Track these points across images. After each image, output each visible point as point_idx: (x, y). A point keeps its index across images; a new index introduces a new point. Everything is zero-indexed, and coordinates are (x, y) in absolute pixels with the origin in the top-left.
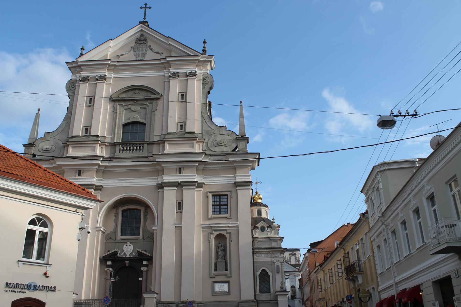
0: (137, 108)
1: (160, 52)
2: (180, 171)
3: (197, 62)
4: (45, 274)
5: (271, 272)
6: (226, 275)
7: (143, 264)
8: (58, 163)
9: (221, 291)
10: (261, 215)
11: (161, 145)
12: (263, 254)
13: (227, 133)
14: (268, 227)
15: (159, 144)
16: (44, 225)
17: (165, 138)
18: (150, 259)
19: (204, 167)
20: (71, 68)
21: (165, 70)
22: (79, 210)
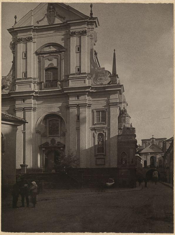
11: (67, 82)
15: (66, 81)
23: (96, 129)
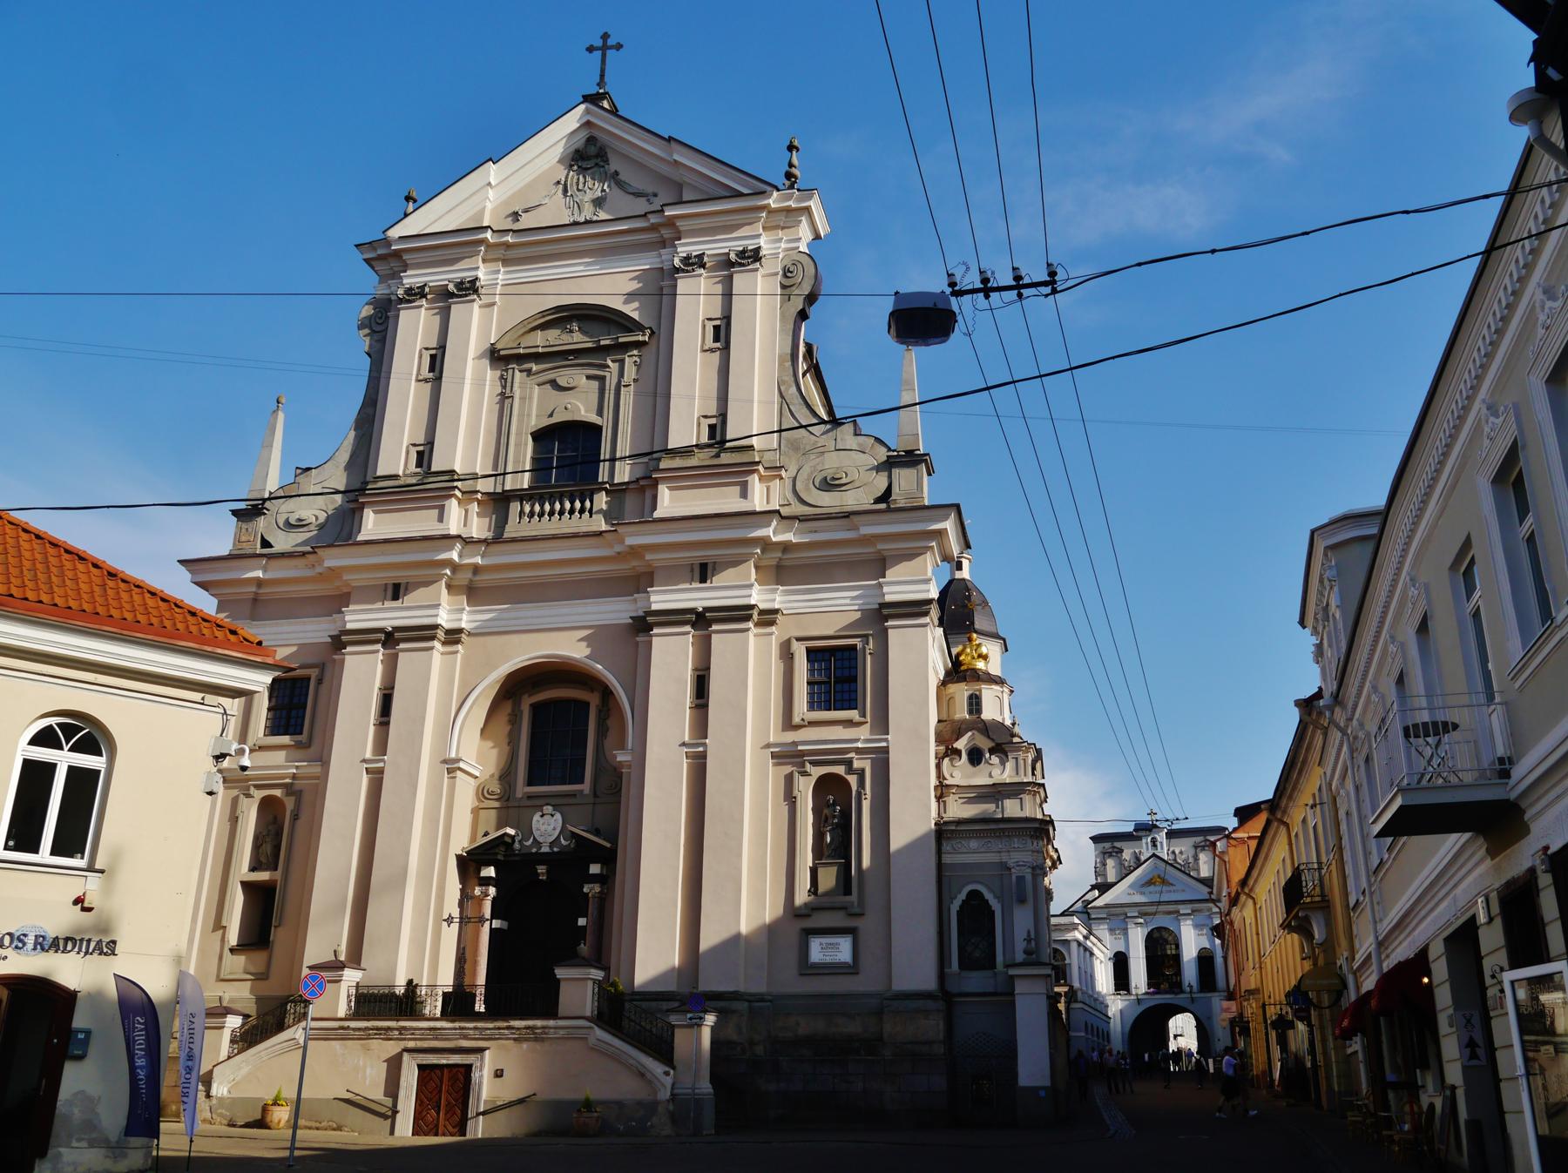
0: (576, 377)
1: (650, 189)
2: (704, 572)
3: (764, 215)
4: (78, 901)
5: (999, 898)
6: (843, 908)
7: (591, 872)
8: (328, 563)
9: (828, 959)
10: (979, 711)
11: (648, 494)
12: (974, 840)
13: (859, 445)
14: (992, 751)
15: (642, 490)
16: (89, 745)
17: (658, 470)
18: (609, 858)
19: (780, 559)
20: (373, 263)
21: (665, 248)
22: (210, 699)
23: (803, 754)
